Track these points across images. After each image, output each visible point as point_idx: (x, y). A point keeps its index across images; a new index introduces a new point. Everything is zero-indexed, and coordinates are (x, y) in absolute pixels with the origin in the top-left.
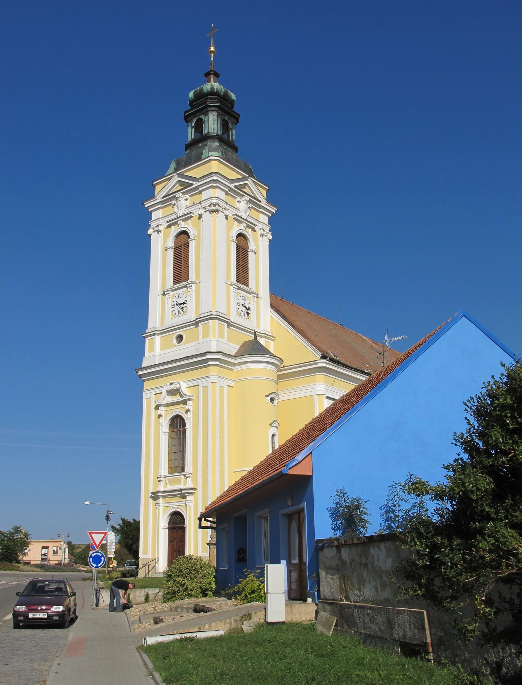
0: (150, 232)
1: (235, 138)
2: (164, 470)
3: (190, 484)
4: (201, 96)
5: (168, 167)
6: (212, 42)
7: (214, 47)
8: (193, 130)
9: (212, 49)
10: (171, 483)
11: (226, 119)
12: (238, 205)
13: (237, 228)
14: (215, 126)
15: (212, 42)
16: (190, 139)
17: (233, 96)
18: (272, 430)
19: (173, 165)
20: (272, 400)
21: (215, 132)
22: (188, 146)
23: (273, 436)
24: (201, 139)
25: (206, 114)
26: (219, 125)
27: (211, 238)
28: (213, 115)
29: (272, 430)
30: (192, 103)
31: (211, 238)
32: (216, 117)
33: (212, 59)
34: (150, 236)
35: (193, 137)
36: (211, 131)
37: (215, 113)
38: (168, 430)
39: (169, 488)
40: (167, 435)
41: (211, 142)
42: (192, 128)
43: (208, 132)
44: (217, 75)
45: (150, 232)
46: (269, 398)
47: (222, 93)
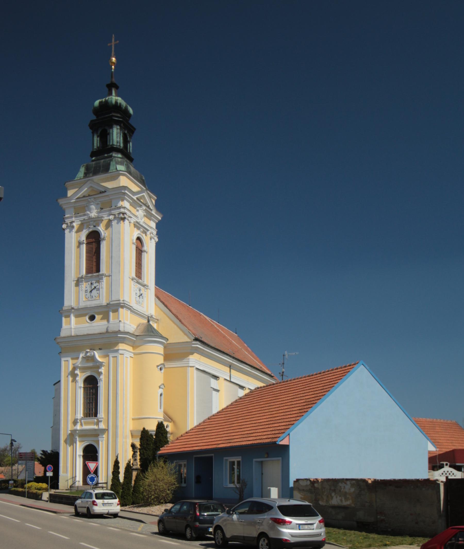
0: (64, 226)
1: (132, 150)
2: (80, 414)
3: (102, 426)
4: (106, 108)
5: (78, 171)
6: (113, 53)
7: (116, 58)
8: (98, 139)
9: (114, 59)
10: (86, 424)
11: (126, 132)
12: (137, 214)
13: (136, 233)
14: (118, 140)
15: (113, 53)
16: (95, 147)
17: (131, 111)
18: (161, 391)
19: (82, 170)
20: (161, 369)
21: (118, 144)
22: (94, 154)
23: (161, 395)
24: (105, 150)
25: (111, 127)
26: (121, 138)
27: (121, 247)
28: (117, 129)
29: (161, 391)
30: (97, 111)
31: (121, 247)
32: (119, 131)
33: (113, 70)
34: (64, 229)
35: (98, 145)
36: (115, 143)
37: (118, 127)
38: (82, 385)
39: (85, 427)
40: (82, 390)
41: (116, 154)
42: (98, 137)
43: (113, 144)
44: (117, 87)
45: (64, 226)
46: (159, 368)
47: (124, 108)
